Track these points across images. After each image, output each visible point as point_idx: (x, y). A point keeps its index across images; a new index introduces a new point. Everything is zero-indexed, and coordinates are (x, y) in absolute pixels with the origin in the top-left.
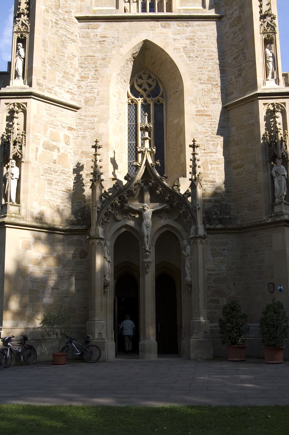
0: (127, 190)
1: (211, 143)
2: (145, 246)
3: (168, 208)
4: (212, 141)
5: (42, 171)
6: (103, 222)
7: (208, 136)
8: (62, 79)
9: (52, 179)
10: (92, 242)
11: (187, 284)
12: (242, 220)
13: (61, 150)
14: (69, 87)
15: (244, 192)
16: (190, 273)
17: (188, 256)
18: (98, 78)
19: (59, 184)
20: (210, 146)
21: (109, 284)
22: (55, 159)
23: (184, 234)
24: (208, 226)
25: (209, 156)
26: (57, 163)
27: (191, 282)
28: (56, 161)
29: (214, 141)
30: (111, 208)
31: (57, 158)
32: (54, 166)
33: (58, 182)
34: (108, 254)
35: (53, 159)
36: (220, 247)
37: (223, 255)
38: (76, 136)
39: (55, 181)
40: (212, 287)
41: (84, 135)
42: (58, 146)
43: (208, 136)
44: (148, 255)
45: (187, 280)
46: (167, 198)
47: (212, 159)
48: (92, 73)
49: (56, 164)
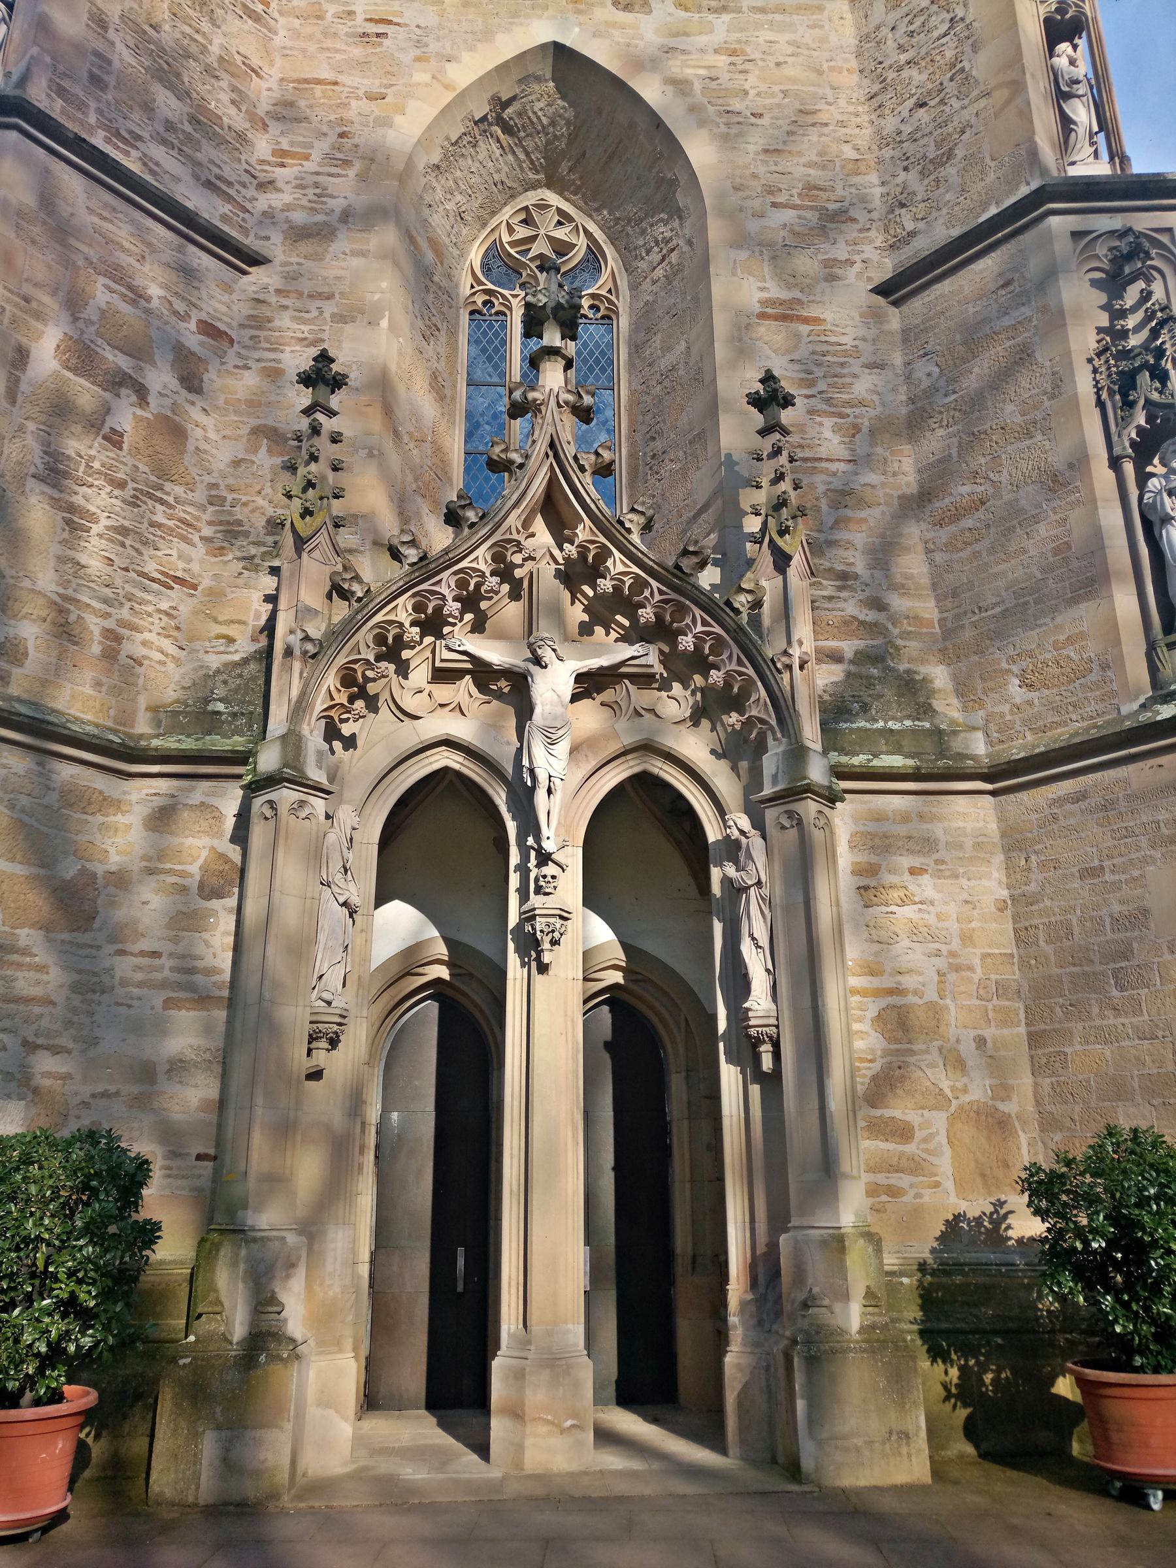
4: (833, 414)
8: (188, 128)
9: (93, 509)
14: (217, 171)
15: (998, 609)
19: (128, 542)
20: (828, 434)
26: (125, 446)
28: (122, 436)
32: (112, 455)
37: (916, 899)
39: (109, 523)
41: (273, 364)
44: (553, 877)
49: (121, 449)
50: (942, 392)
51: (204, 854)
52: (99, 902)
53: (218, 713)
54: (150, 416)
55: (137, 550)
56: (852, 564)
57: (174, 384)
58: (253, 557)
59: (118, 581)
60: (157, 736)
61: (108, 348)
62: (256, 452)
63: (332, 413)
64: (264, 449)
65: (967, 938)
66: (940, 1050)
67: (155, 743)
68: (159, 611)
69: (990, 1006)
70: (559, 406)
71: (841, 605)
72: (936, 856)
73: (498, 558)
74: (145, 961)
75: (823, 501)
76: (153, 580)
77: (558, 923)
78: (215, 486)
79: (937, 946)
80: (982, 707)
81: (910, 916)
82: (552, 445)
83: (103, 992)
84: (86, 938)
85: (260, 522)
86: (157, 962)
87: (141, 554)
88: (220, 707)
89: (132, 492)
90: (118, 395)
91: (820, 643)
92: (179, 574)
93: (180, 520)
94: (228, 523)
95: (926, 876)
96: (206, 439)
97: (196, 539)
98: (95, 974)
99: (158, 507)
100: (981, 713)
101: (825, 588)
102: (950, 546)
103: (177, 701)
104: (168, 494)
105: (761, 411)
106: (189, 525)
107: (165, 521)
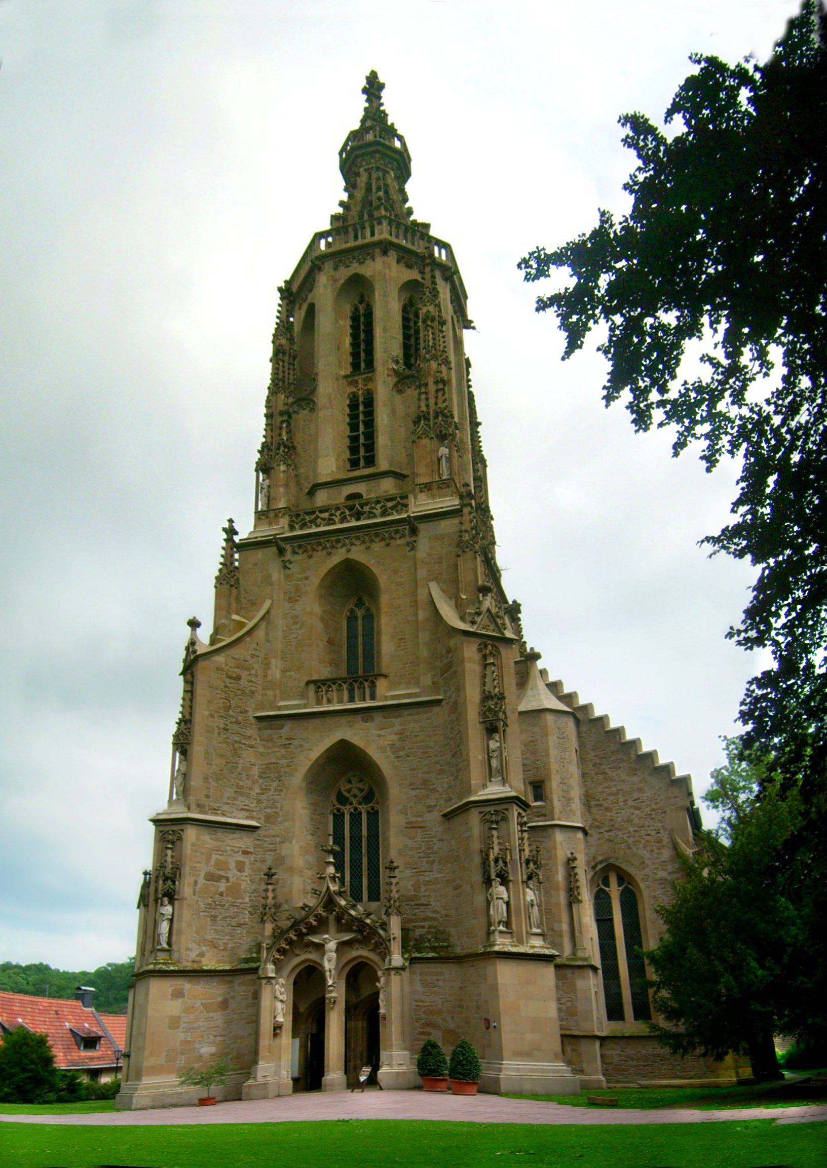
1: (425, 860)
13: (231, 880)
18: (281, 790)
20: (424, 864)
33: (226, 917)
48: (275, 784)
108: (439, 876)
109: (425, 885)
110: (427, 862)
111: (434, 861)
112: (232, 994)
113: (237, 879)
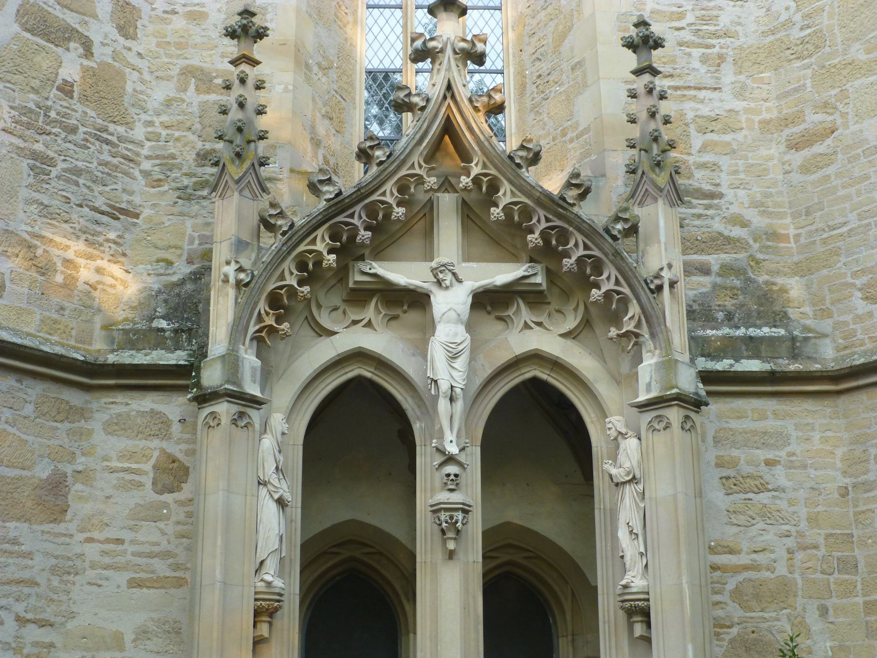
0: (366, 201)
1: (696, 52)
2: (441, 435)
3: (540, 284)
4: (699, 46)
5: (6, 116)
6: (260, 331)
7: (683, 28)
10: (212, 413)
11: (628, 604)
12: (840, 341)
13: (96, 50)
15: (845, 229)
16: (641, 554)
17: (629, 481)
20: (696, 64)
21: (279, 601)
22: (69, 80)
23: (604, 389)
24: (703, 363)
25: (690, 99)
26: (75, 95)
27: (646, 596)
28: (72, 86)
29: (708, 47)
30: (295, 272)
31: (77, 78)
32: (65, 104)
34: (277, 468)
35: (60, 77)
36: (758, 451)
37: (770, 487)
38: (165, 12)
40: (728, 624)
41: (197, 8)
42: (86, 34)
43: (683, 28)
44: (456, 476)
45: (625, 587)
46: (534, 238)
47: (705, 110)
49: (72, 98)
50: (798, 26)
51: (156, 454)
52: (70, 497)
53: (163, 330)
54: (94, 65)
55: (88, 187)
56: (718, 185)
57: (114, 34)
58: (186, 187)
59: (74, 216)
60: (113, 351)
61: (58, 7)
62: (185, 90)
63: (254, 63)
64: (192, 87)
65: (813, 520)
66: (789, 617)
67: (112, 358)
68: (108, 240)
69: (832, 579)
70: (455, 53)
71: (708, 222)
72: (789, 449)
73: (402, 188)
74: (111, 547)
75: (692, 126)
76: (103, 213)
77: (459, 516)
78: (150, 123)
79: (787, 527)
80: (830, 316)
81: (765, 502)
82: (449, 87)
83: (77, 574)
84: (61, 528)
85: (191, 157)
86: (120, 547)
87: (92, 190)
88: (163, 324)
89: (82, 136)
90: (68, 49)
91: (687, 258)
92: (123, 206)
93: (125, 157)
94: (164, 158)
95: (779, 467)
96: (143, 82)
97: (137, 173)
98: (69, 559)
99: (105, 146)
100: (830, 321)
101: (694, 207)
102: (805, 169)
103: (126, 319)
104: (112, 134)
105: (634, 52)
106: (131, 160)
107: (110, 159)
108: (739, 105)
109: (703, 131)
110: (704, 59)
111: (722, 58)
112: (81, 462)
113: (115, 55)
